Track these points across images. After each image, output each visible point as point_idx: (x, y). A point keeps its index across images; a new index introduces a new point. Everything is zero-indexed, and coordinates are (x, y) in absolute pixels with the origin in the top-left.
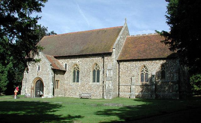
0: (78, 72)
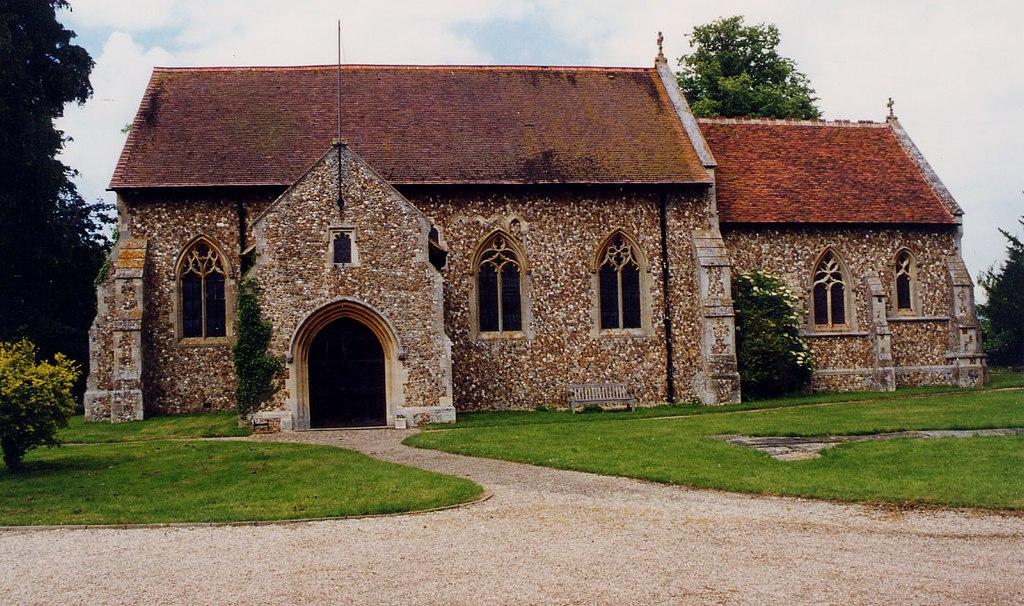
0: (511, 273)
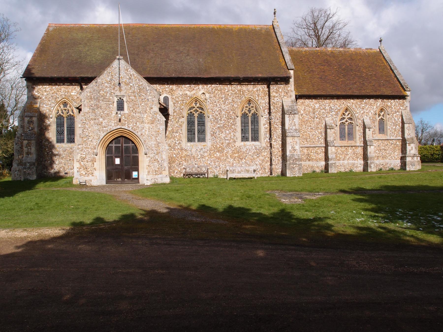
0: (201, 117)
